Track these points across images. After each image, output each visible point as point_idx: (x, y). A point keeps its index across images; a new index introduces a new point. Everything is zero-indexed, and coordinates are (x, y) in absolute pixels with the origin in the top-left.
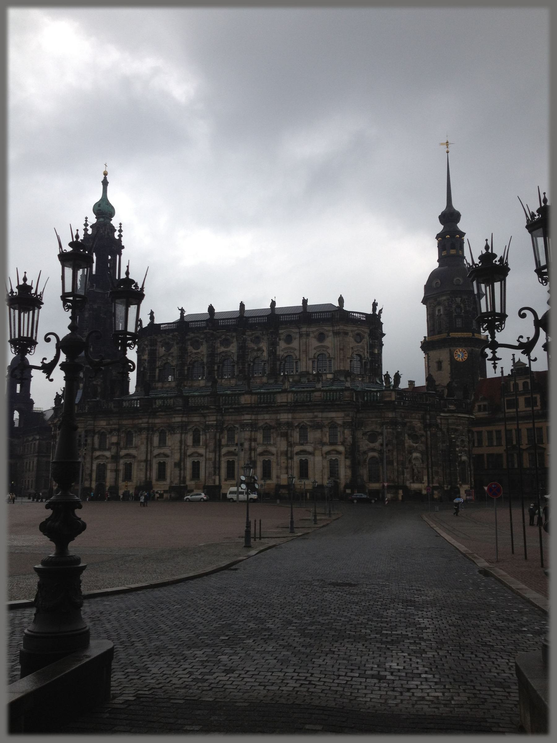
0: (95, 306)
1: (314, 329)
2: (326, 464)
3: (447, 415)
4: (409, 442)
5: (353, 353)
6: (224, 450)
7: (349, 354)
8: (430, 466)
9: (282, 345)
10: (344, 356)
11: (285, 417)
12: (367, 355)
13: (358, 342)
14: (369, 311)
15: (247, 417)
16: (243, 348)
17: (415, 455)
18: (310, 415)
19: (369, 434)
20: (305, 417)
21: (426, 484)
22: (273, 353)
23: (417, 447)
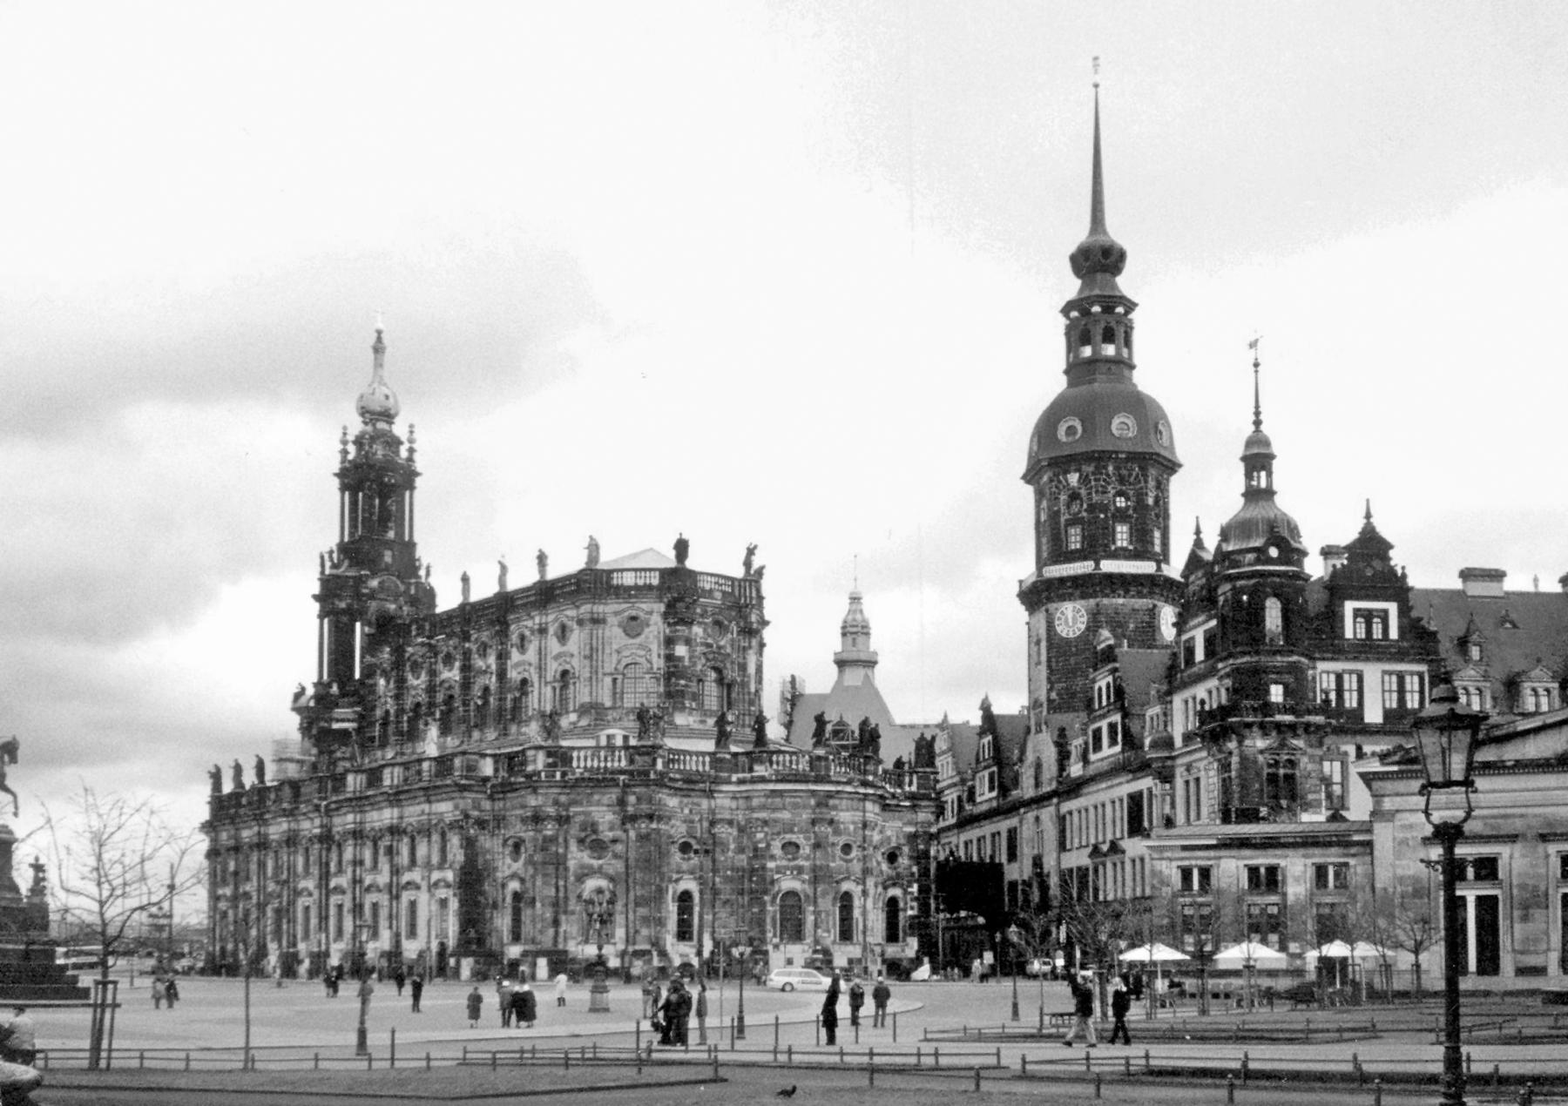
0: (343, 605)
1: (551, 618)
2: (435, 907)
3: (743, 788)
4: (577, 857)
5: (619, 662)
6: (332, 884)
7: (609, 668)
8: (631, 905)
9: (515, 656)
10: (594, 671)
11: (384, 816)
12: (659, 663)
13: (633, 637)
14: (670, 561)
15: (350, 817)
16: (466, 668)
17: (592, 884)
18: (418, 809)
19: (510, 842)
20: (414, 813)
21: (621, 947)
22: (502, 674)
23: (601, 867)
